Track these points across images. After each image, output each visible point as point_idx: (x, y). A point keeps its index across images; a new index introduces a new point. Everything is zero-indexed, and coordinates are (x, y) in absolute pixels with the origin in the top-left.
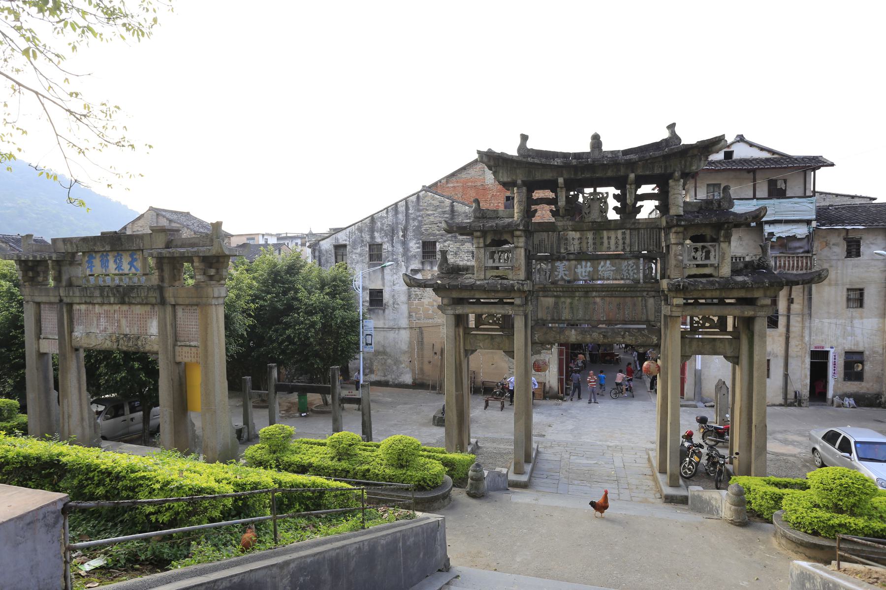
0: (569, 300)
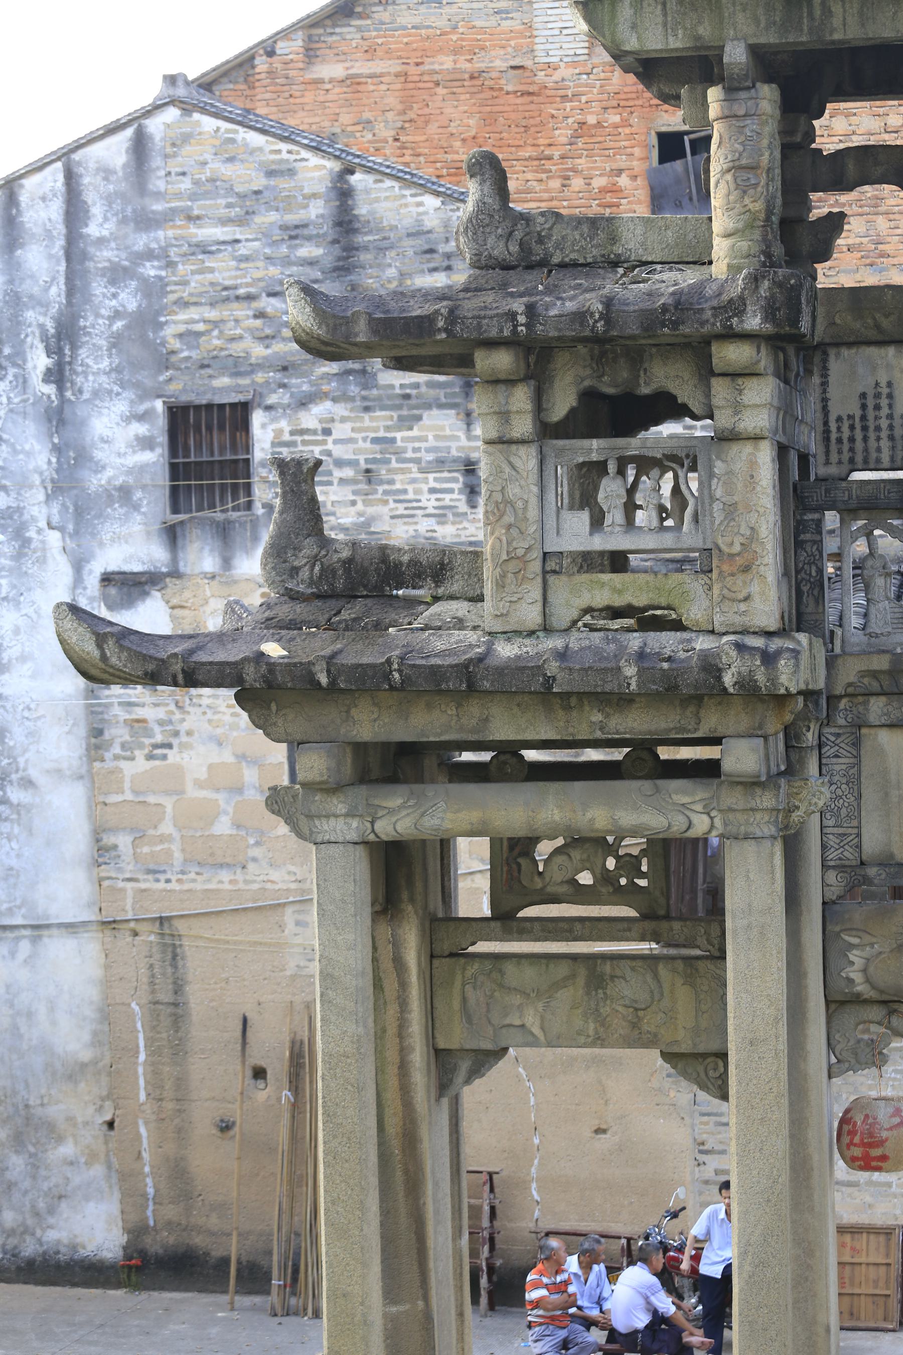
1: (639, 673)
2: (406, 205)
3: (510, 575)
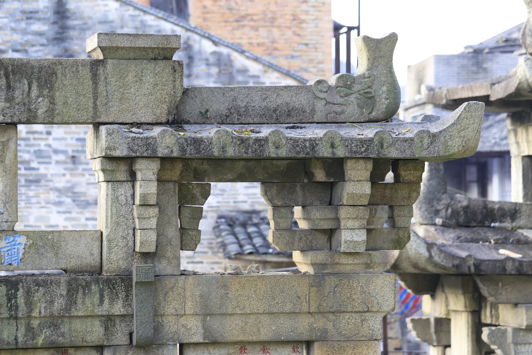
2: (98, 5)
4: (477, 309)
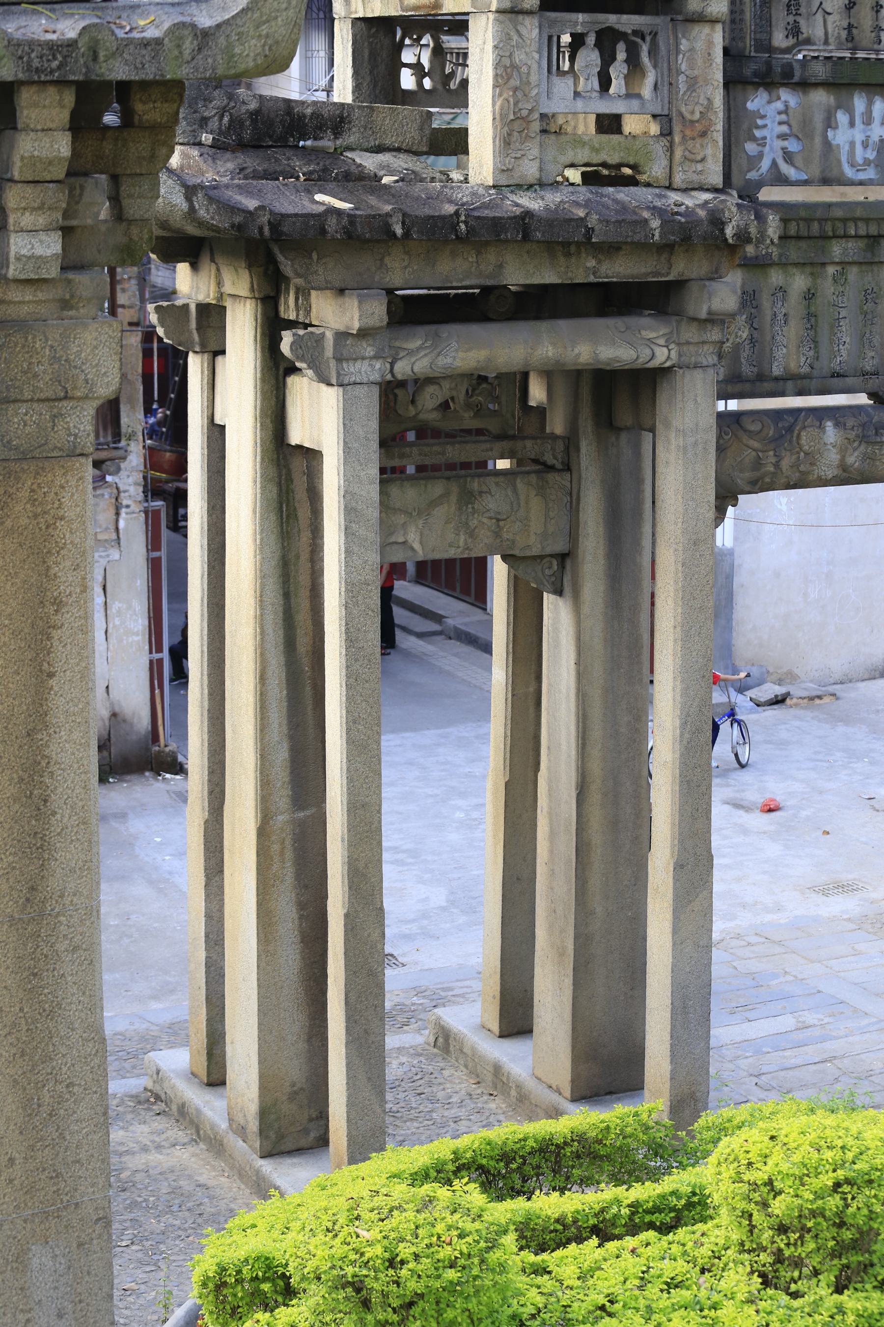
0: (799, 282)
1: (661, 226)
3: (515, 134)
4: (272, 294)
